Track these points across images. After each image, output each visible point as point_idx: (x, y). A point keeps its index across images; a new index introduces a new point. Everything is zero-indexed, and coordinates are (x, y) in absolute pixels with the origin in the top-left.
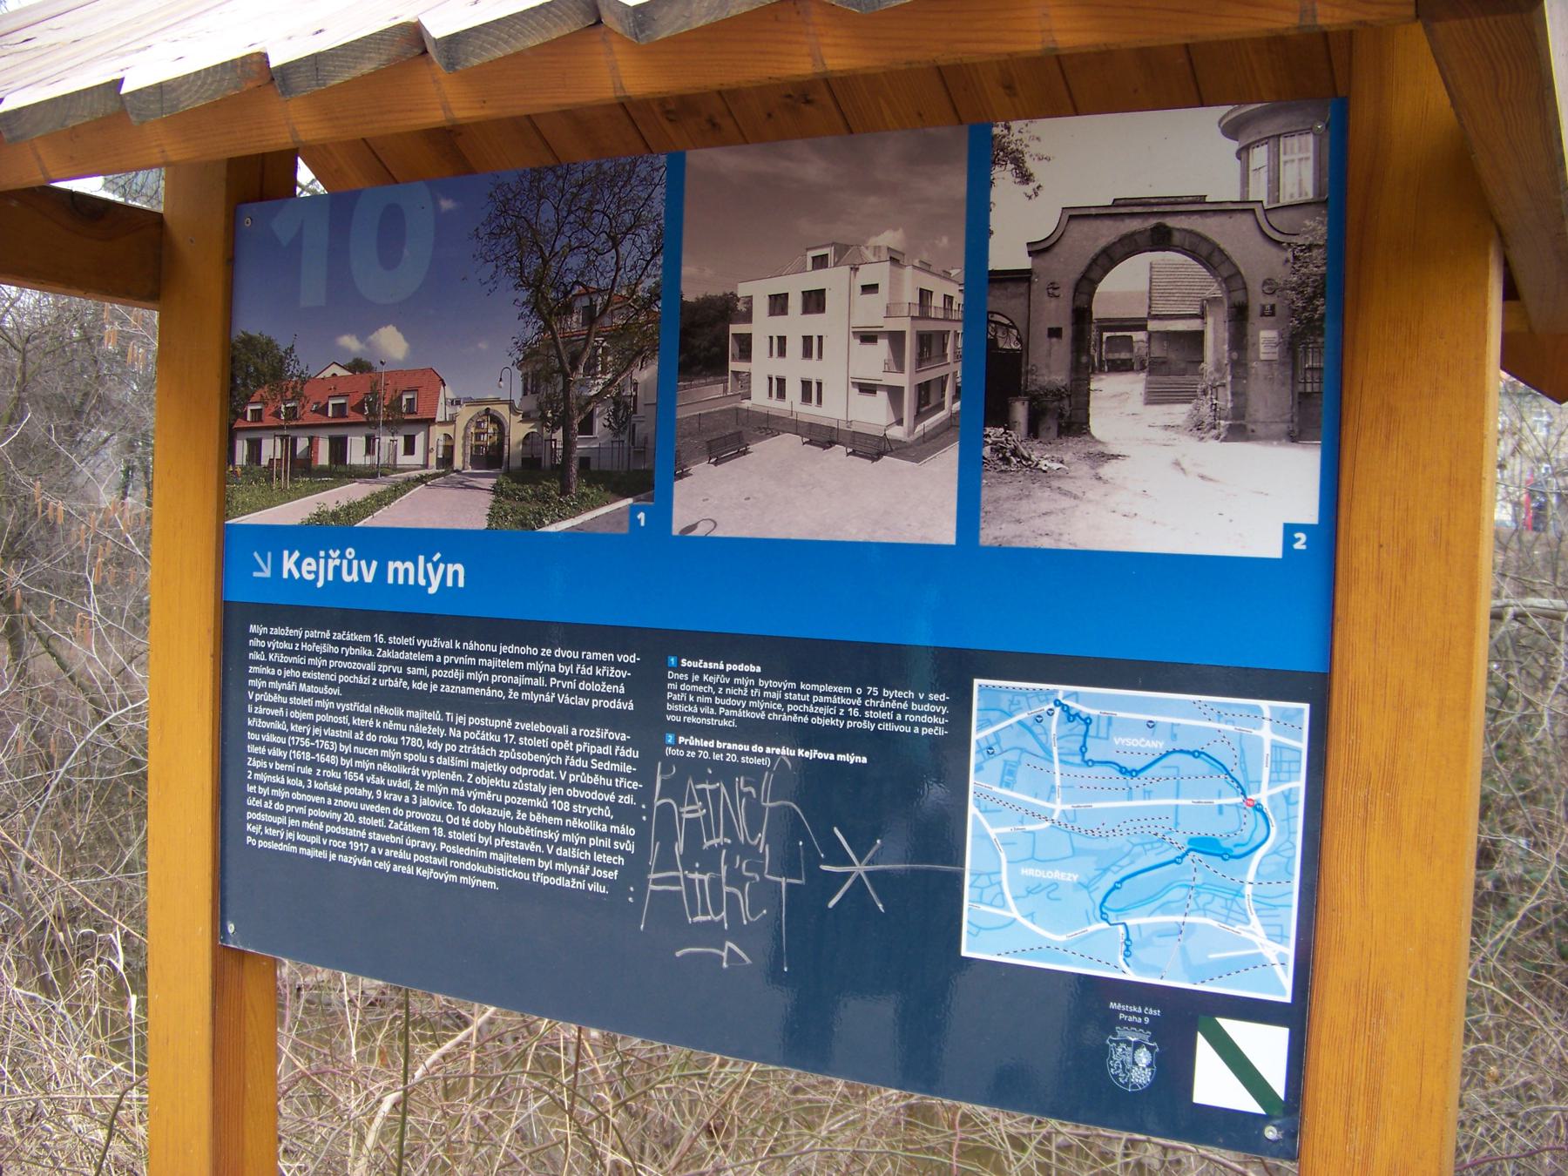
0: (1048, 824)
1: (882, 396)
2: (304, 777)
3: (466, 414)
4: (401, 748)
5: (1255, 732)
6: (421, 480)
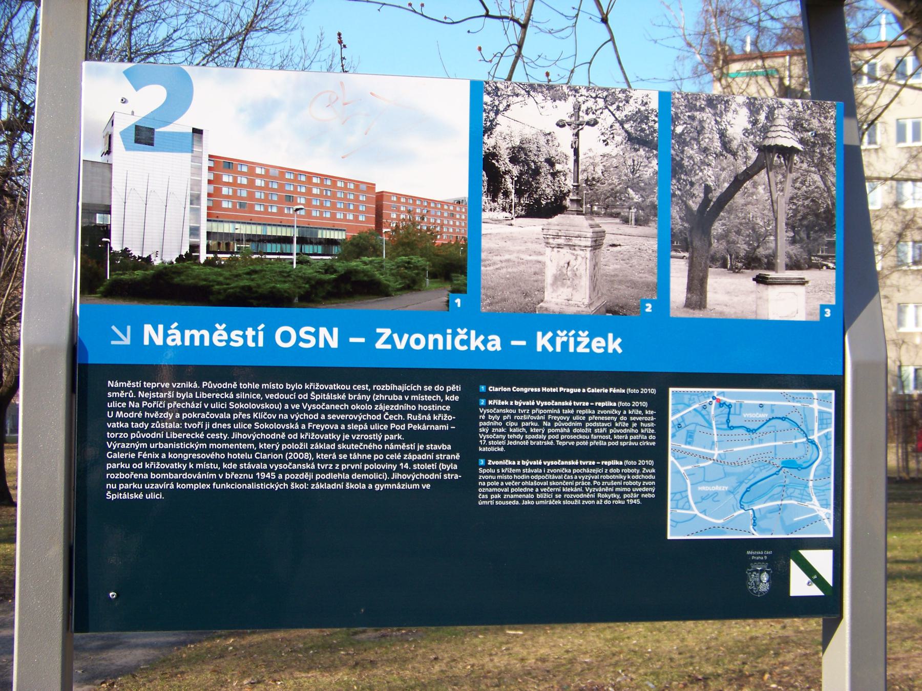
0: (711, 462)
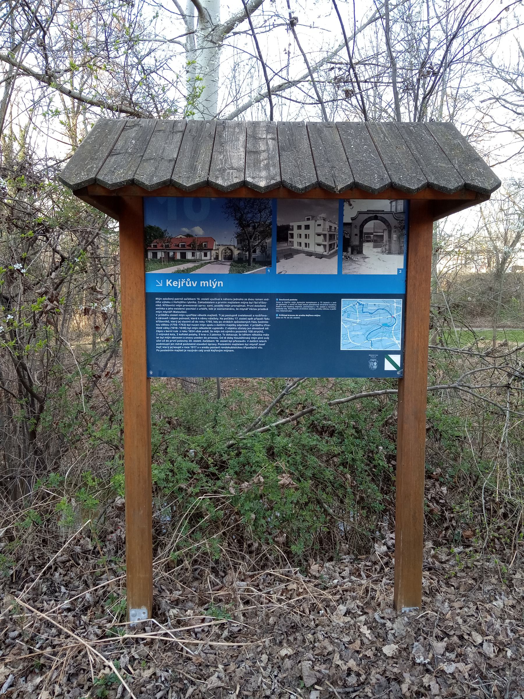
1: (322, 246)
2: (176, 333)
3: (221, 248)
4: (205, 323)
6: (209, 263)
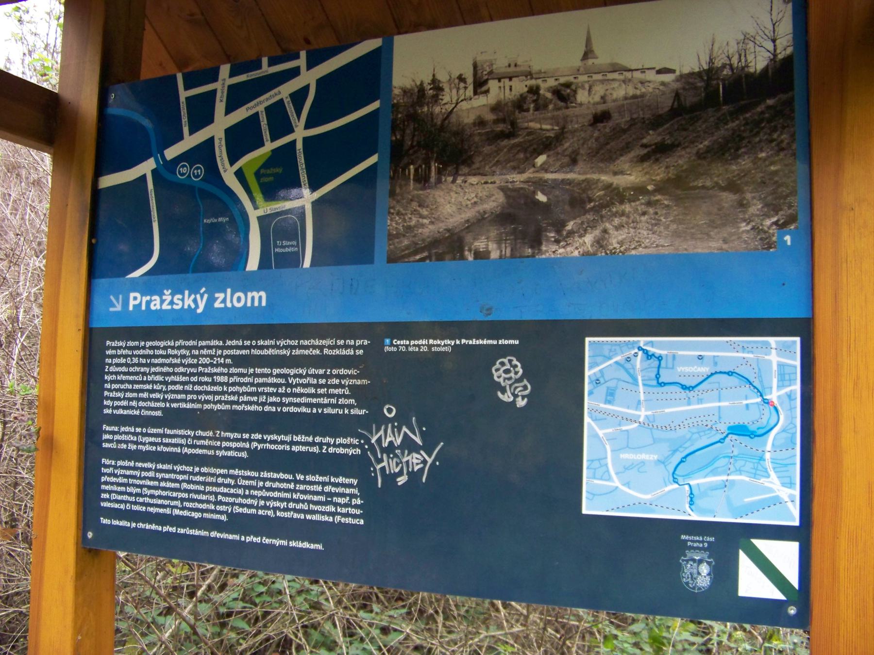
0: (636, 425)
5: (767, 357)
